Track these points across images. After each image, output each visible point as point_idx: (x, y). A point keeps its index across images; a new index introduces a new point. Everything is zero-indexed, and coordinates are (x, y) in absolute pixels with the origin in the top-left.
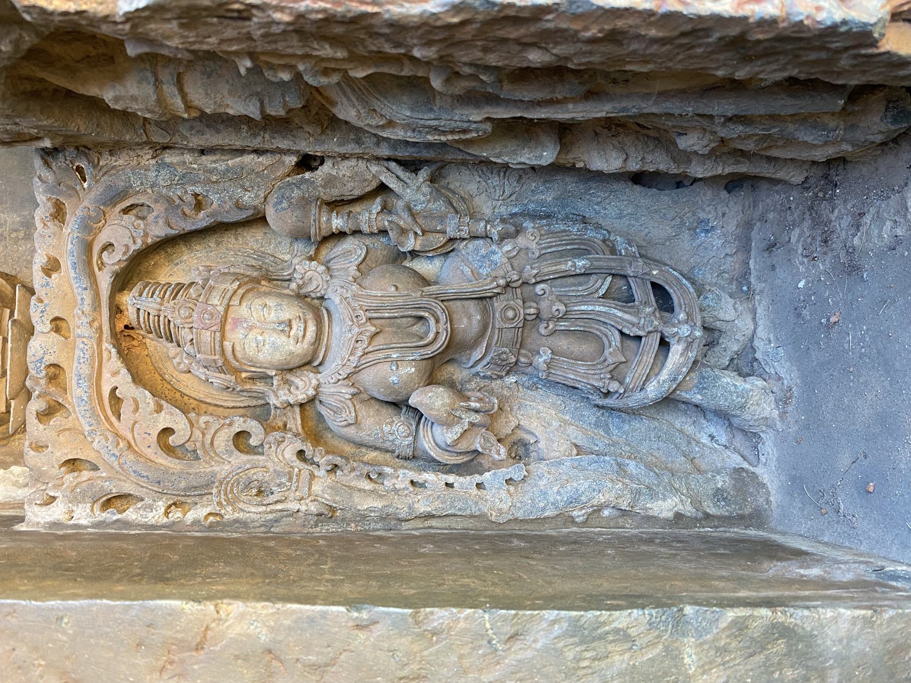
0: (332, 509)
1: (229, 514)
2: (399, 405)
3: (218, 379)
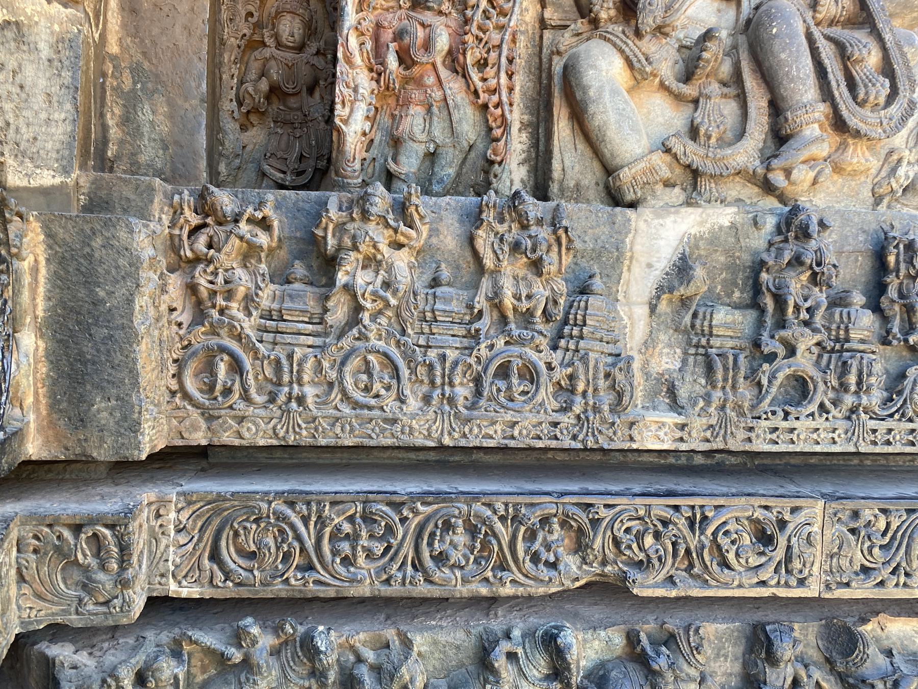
0: (224, 45)
1: (224, 7)
2: (262, 74)
3: (273, 10)
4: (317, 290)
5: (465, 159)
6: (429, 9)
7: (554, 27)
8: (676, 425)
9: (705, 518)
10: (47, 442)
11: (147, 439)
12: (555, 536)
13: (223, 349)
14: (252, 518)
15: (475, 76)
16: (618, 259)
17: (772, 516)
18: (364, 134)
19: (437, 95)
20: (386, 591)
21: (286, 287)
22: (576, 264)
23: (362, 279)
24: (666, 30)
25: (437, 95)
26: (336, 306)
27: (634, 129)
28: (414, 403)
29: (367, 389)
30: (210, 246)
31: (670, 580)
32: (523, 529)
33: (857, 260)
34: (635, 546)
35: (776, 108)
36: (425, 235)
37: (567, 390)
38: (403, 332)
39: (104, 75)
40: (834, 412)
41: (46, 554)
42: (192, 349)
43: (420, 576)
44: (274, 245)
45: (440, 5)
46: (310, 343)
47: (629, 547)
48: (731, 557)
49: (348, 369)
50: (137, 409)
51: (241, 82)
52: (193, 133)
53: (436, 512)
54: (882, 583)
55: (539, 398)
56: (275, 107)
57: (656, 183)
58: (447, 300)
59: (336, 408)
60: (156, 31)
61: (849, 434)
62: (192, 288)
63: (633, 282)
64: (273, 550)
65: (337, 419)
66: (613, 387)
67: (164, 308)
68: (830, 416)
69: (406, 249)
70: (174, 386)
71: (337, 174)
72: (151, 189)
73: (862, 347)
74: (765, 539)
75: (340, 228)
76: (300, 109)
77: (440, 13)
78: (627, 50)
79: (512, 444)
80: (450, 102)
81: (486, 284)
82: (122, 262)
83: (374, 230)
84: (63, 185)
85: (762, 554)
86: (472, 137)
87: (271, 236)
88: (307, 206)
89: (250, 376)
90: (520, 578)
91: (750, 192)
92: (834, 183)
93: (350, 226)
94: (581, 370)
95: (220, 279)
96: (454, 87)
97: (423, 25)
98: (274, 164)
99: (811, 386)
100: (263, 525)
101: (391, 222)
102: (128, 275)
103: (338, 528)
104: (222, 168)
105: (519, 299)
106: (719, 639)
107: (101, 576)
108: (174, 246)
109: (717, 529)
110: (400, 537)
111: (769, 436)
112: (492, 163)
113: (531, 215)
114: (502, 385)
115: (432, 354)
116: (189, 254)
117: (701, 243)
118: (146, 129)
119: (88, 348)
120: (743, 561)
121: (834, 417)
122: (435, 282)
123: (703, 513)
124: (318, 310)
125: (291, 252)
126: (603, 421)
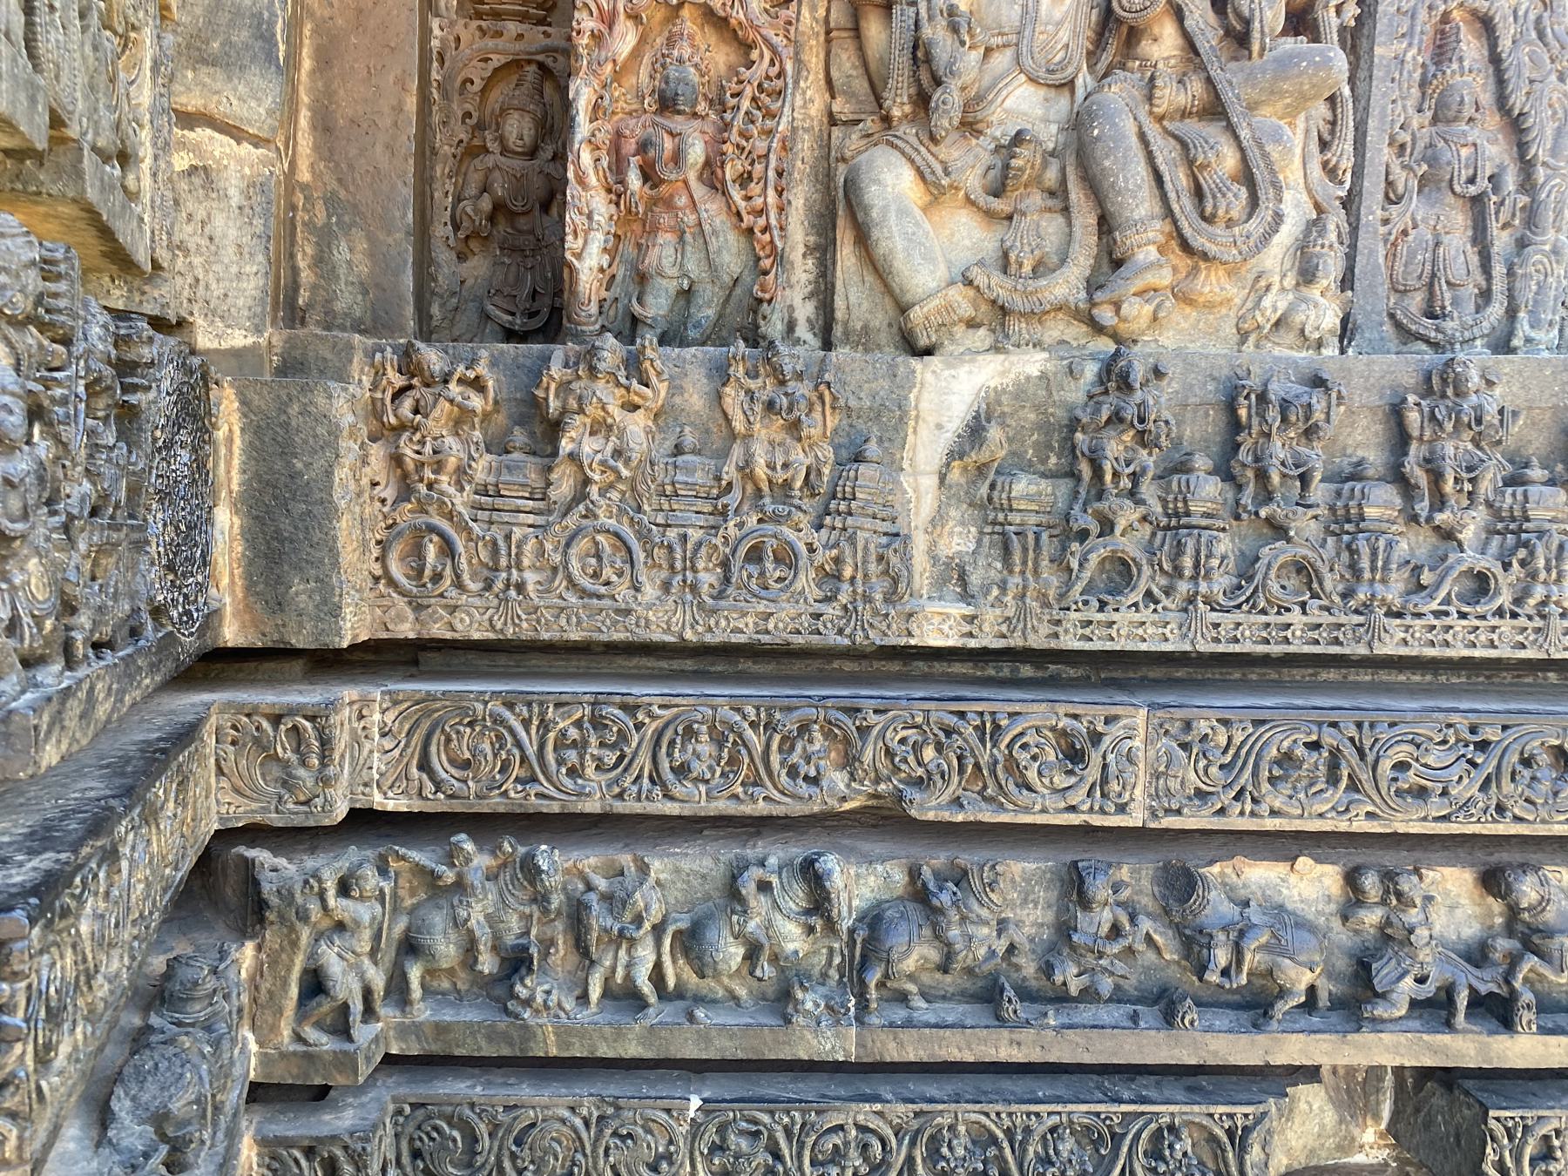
1: (435, 108)
3: (497, 107)
4: (538, 460)
5: (730, 295)
6: (679, 113)
7: (845, 123)
8: (964, 617)
9: (997, 727)
10: (243, 626)
11: (349, 625)
12: (817, 746)
13: (432, 529)
14: (467, 720)
15: (736, 194)
16: (901, 418)
17: (1082, 727)
18: (602, 270)
19: (691, 219)
20: (620, 807)
21: (504, 457)
22: (851, 426)
23: (589, 446)
24: (979, 126)
25: (691, 219)
26: (560, 479)
27: (929, 258)
28: (650, 592)
29: (596, 575)
30: (416, 411)
31: (957, 802)
32: (777, 738)
33: (1207, 415)
34: (911, 758)
35: (1106, 225)
36: (663, 394)
37: (834, 576)
38: (639, 509)
39: (294, 208)
40: (1165, 602)
41: (245, 745)
42: (397, 529)
43: (658, 791)
44: (489, 408)
45: (694, 106)
46: (530, 522)
47: (905, 760)
48: (1032, 775)
49: (573, 551)
50: (337, 591)
51: (458, 199)
52: (397, 273)
53: (676, 717)
54: (1222, 811)
55: (798, 586)
56: (501, 228)
57: (954, 324)
58: (690, 471)
59: (561, 597)
60: (353, 152)
61: (1184, 629)
62: (397, 460)
63: (920, 447)
64: (490, 757)
65: (562, 609)
66: (886, 572)
67: (365, 481)
68: (1159, 607)
69: (642, 411)
70: (378, 572)
71: (569, 321)
72: (350, 347)
73: (1204, 522)
74: (1074, 756)
75: (564, 387)
76: (532, 232)
77: (695, 115)
78: (918, 159)
79: (765, 639)
80: (707, 228)
81: (737, 452)
82: (320, 430)
83: (602, 389)
84: (256, 346)
85: (1070, 773)
86: (736, 269)
87: (486, 398)
88: (528, 362)
89: (463, 560)
90: (777, 795)
91: (1076, 332)
92: (1186, 318)
93: (574, 386)
94: (848, 551)
95: (428, 449)
96: (712, 210)
97: (671, 133)
98: (500, 303)
99: (1134, 570)
100: (478, 729)
101: (623, 380)
102: (327, 444)
103: (563, 734)
104: (435, 310)
105: (774, 469)
106: (1028, 881)
107: (301, 772)
108: (376, 411)
109: (1013, 741)
110: (634, 745)
111: (1080, 631)
112: (760, 301)
113: (787, 369)
114: (753, 569)
115: (672, 534)
116: (393, 420)
117: (1004, 399)
118: (342, 271)
119: (285, 525)
120: (1046, 781)
121: (1164, 608)
122: (678, 450)
123: (994, 722)
124: (540, 484)
125: (510, 417)
126: (876, 612)
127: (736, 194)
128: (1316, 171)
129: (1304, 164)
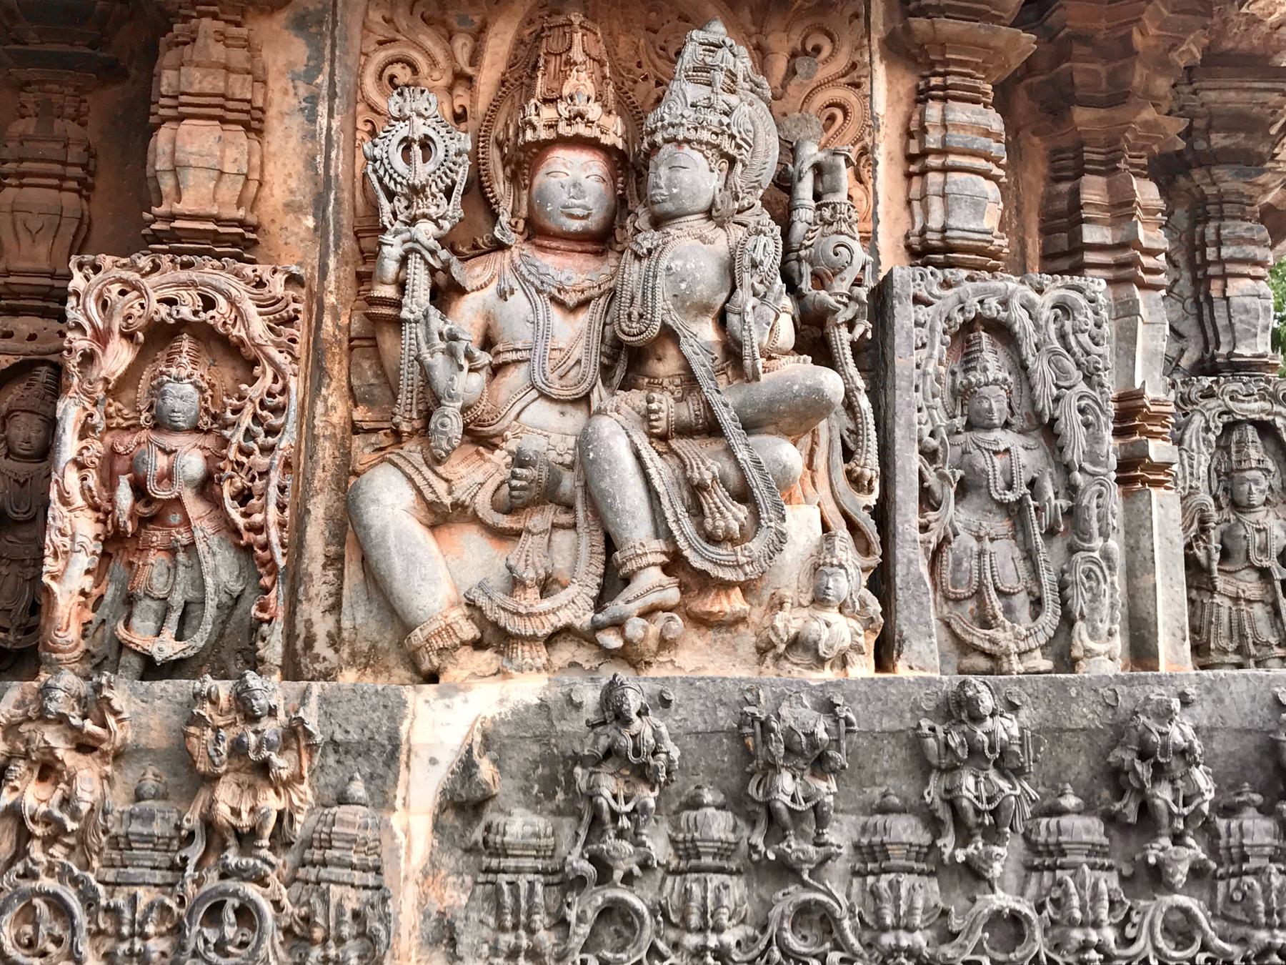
127: (235, 514)
128: (842, 483)
129: (830, 474)
